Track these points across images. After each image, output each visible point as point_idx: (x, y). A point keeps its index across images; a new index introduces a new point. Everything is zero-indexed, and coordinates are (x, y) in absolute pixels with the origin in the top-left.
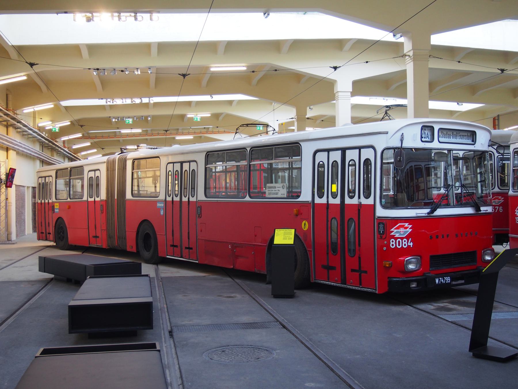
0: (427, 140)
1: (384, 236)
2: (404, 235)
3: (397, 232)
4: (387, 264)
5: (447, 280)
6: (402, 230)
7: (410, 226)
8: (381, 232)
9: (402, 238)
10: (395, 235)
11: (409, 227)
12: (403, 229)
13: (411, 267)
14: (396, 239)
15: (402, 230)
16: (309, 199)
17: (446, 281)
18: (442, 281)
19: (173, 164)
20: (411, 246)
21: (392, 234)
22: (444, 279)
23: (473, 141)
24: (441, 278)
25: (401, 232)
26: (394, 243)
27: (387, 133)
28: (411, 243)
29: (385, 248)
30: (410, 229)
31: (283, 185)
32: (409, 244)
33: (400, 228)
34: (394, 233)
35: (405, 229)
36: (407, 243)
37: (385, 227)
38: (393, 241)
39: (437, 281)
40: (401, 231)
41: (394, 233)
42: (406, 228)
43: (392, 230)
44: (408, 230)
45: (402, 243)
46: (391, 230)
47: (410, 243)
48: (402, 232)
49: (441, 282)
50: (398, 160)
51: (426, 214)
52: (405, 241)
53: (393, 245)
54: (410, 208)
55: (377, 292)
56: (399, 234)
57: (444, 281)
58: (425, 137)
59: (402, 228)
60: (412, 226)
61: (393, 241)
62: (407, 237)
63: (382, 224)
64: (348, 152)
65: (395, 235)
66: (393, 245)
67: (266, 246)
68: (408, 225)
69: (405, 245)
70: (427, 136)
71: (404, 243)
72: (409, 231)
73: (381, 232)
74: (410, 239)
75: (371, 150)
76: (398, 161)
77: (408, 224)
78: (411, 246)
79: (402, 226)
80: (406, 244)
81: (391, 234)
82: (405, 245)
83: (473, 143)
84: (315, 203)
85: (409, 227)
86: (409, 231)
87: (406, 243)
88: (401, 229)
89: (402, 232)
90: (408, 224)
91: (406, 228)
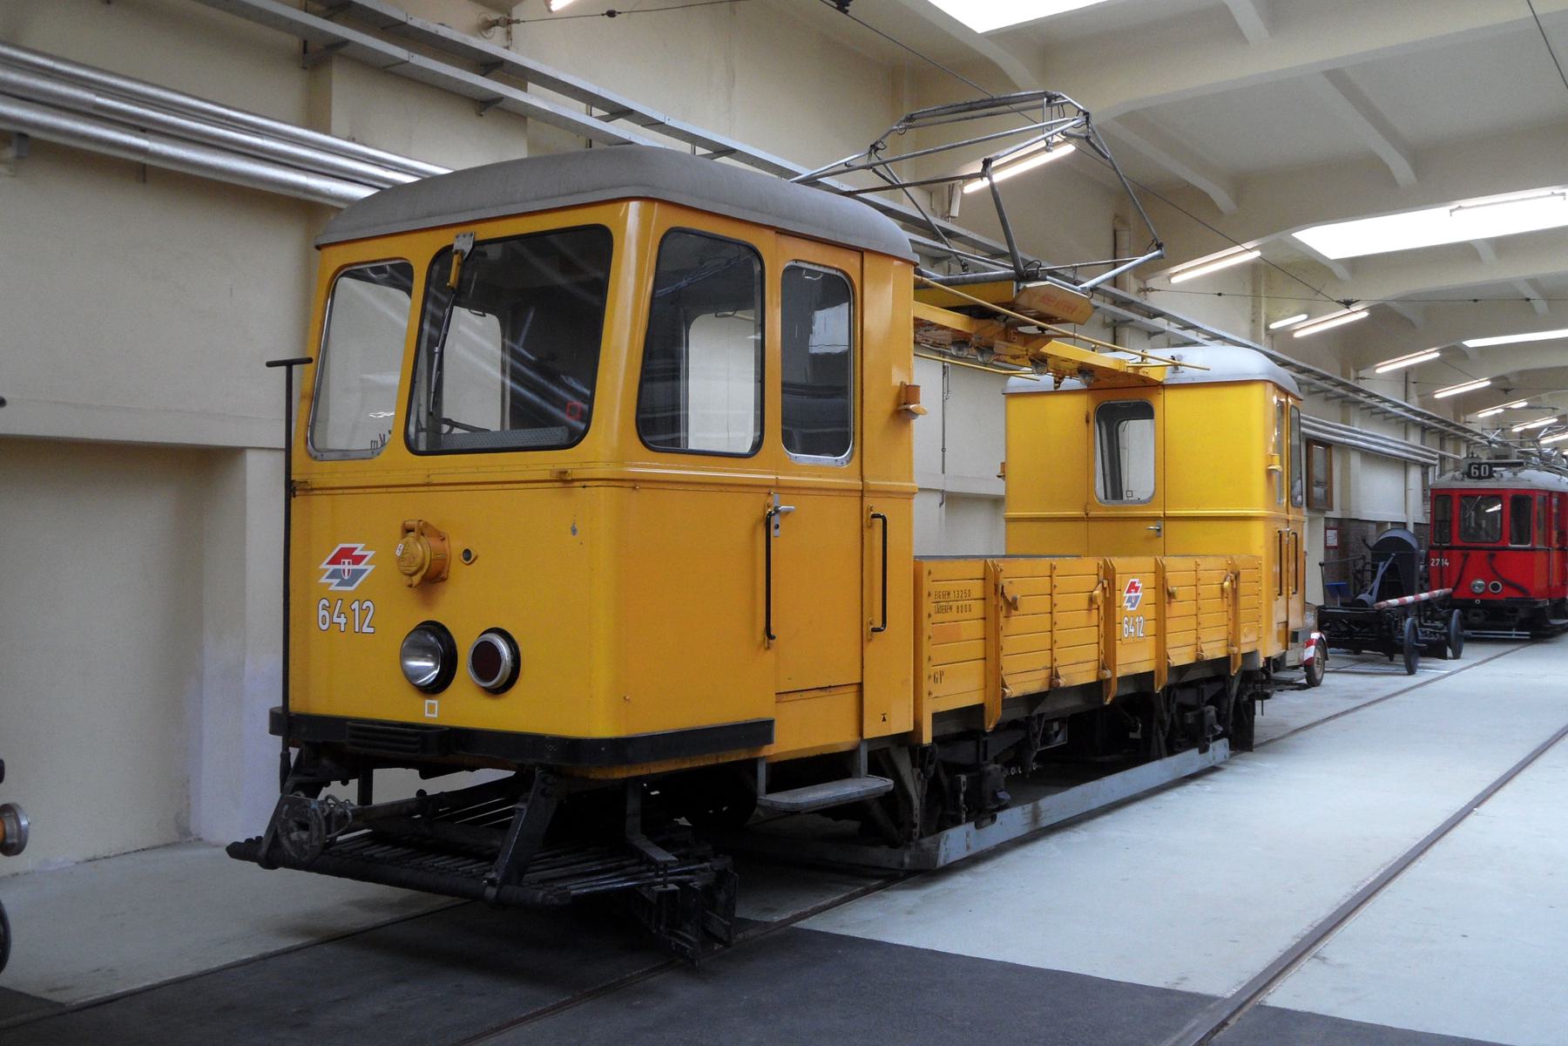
2: (351, 586)
3: (334, 575)
11: (365, 556)
12: (349, 563)
15: (347, 567)
35: (353, 564)
40: (344, 570)
42: (358, 560)
44: (361, 566)
48: (346, 572)
56: (339, 580)
59: (347, 561)
85: (365, 556)
88: (344, 563)
89: (346, 572)
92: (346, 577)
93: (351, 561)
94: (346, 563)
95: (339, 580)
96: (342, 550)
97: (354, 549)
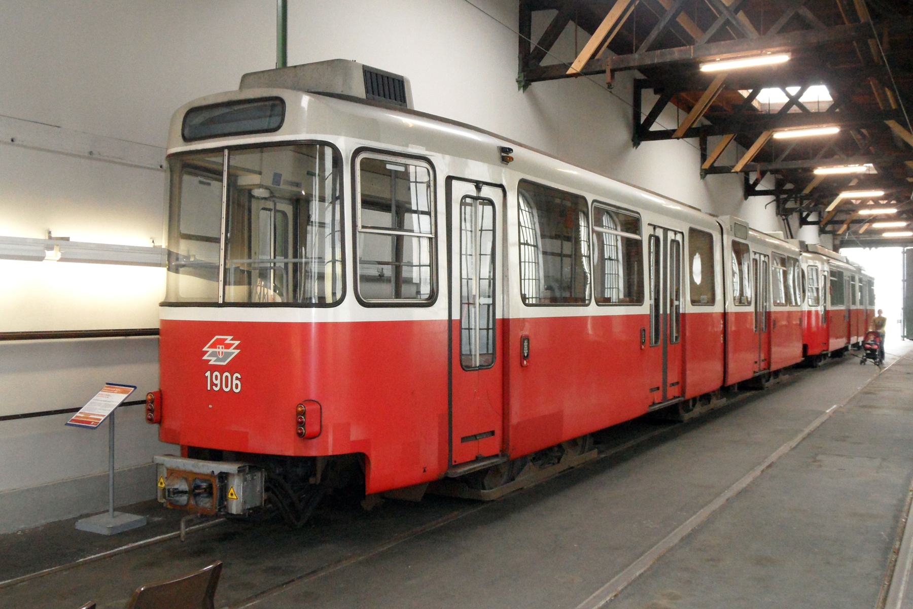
2: (224, 362)
6: (220, 349)
7: (237, 343)
9: (221, 369)
10: (210, 360)
11: (234, 344)
15: (221, 350)
21: (205, 358)
25: (219, 354)
30: (236, 348)
33: (218, 346)
35: (226, 348)
40: (219, 352)
42: (228, 346)
43: (205, 349)
44: (231, 350)
48: (221, 353)
59: (221, 346)
60: (239, 342)
62: (231, 368)
65: (210, 360)
72: (233, 353)
77: (232, 337)
79: (221, 342)
85: (234, 344)
86: (233, 353)
88: (219, 348)
89: (221, 353)
90: (232, 337)
91: (228, 346)
92: (221, 357)
93: (223, 346)
94: (221, 348)
95: (215, 358)
96: (217, 340)
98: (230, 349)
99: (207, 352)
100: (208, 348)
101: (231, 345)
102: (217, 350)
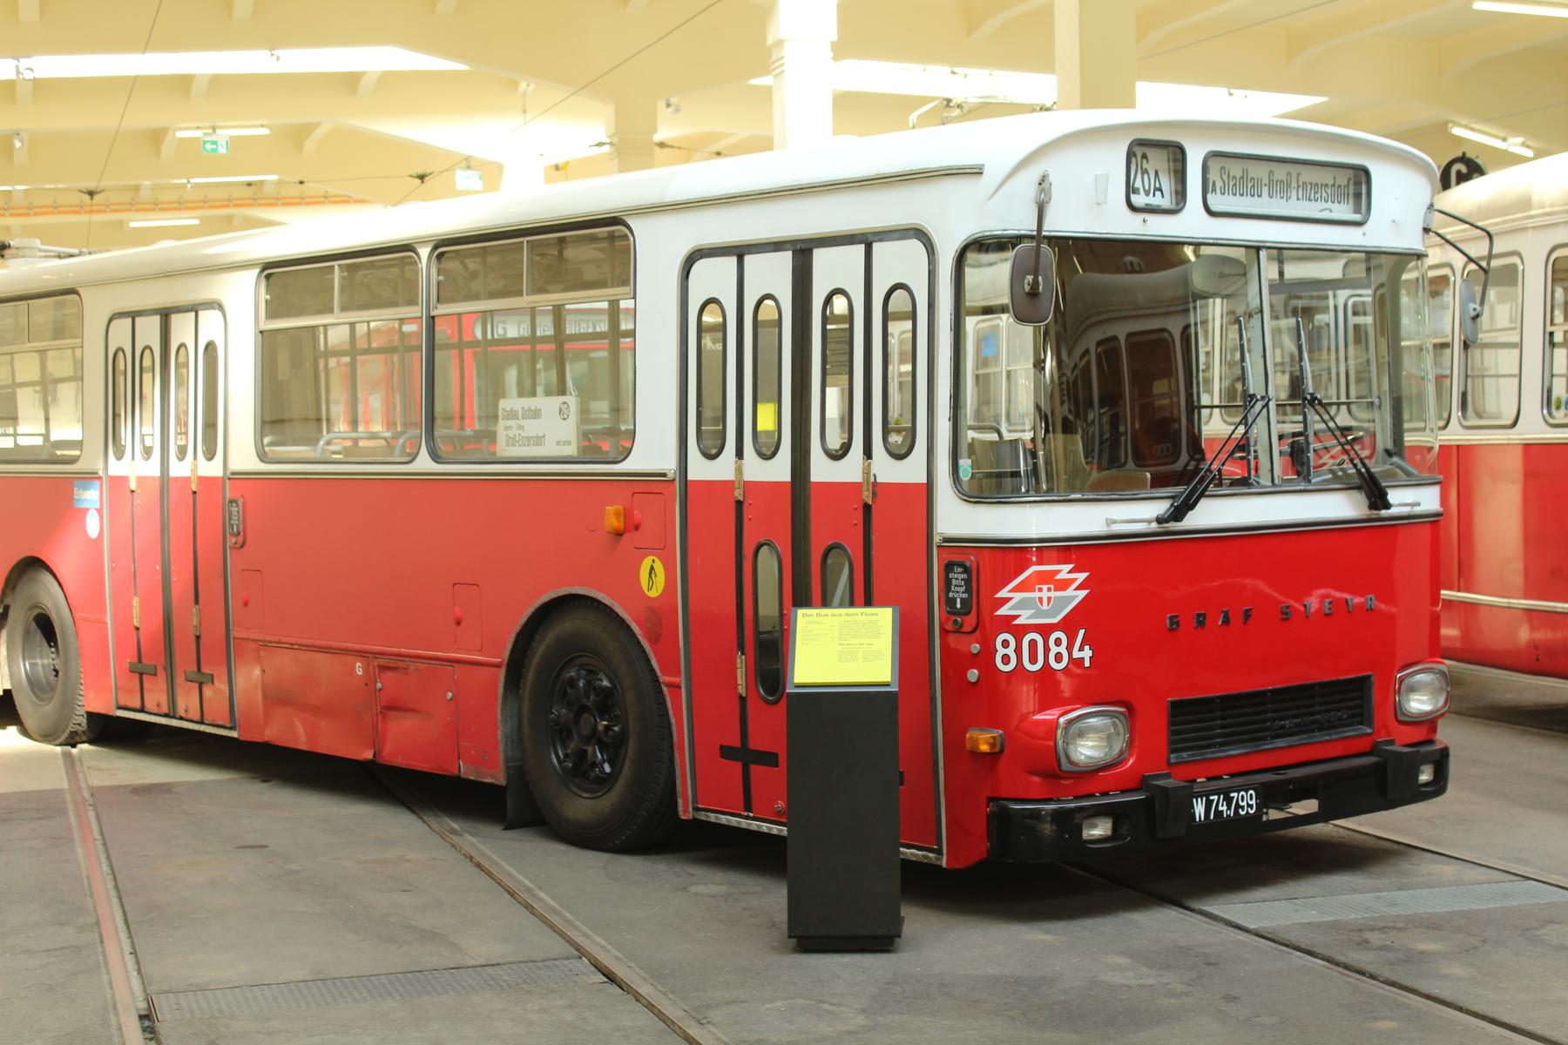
0: (1156, 200)
1: (970, 622)
2: (1054, 617)
3: (1022, 604)
4: (983, 740)
5: (1244, 803)
6: (1045, 592)
7: (1082, 576)
8: (958, 606)
9: (1045, 630)
10: (1017, 617)
11: (1073, 580)
12: (1049, 590)
13: (1087, 750)
14: (1020, 632)
16: (669, 464)
17: (1237, 805)
18: (1220, 808)
19: (130, 320)
20: (1087, 664)
22: (1229, 800)
23: (1357, 210)
24: (1216, 797)
25: (1041, 604)
26: (1011, 651)
27: (977, 172)
28: (1087, 647)
29: (973, 675)
30: (1077, 589)
31: (564, 403)
32: (1076, 654)
33: (1037, 587)
34: (1010, 609)
35: (1055, 590)
36: (1070, 648)
37: (974, 585)
38: (1006, 644)
39: (1199, 809)
40: (1041, 599)
41: (1010, 609)
42: (1063, 585)
43: (1003, 594)
44: (1070, 592)
45: (1047, 650)
46: (998, 595)
47: (1081, 649)
48: (1045, 601)
49: (1218, 813)
50: (1027, 288)
51: (1149, 522)
52: (1058, 642)
53: (1006, 660)
54: (1078, 496)
55: (944, 865)
57: (1229, 808)
58: (1147, 188)
59: (1045, 587)
61: (1006, 644)
62: (1068, 625)
63: (960, 570)
64: (820, 256)
65: (1017, 617)
66: (1006, 660)
67: (498, 666)
68: (1070, 572)
69: (1058, 658)
70: (1157, 185)
71: (1054, 649)
73: (958, 606)
74: (1082, 632)
75: (915, 247)
76: (1028, 294)
77: (1071, 566)
78: (1087, 664)
80: (1062, 653)
81: (998, 613)
82: (1058, 658)
83: (1357, 217)
84: (689, 479)
85: (1073, 580)
86: (1075, 597)
87: (1063, 649)
88: (1040, 590)
89: (1045, 601)
93: (1052, 586)
97: (1059, 572)
98: (1068, 590)
99: (1006, 600)
100: (1013, 590)
101: (1070, 582)
102: (1037, 595)
